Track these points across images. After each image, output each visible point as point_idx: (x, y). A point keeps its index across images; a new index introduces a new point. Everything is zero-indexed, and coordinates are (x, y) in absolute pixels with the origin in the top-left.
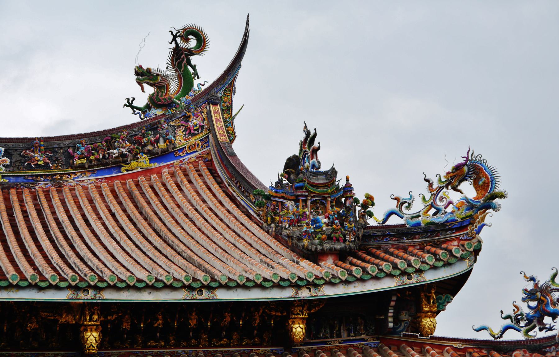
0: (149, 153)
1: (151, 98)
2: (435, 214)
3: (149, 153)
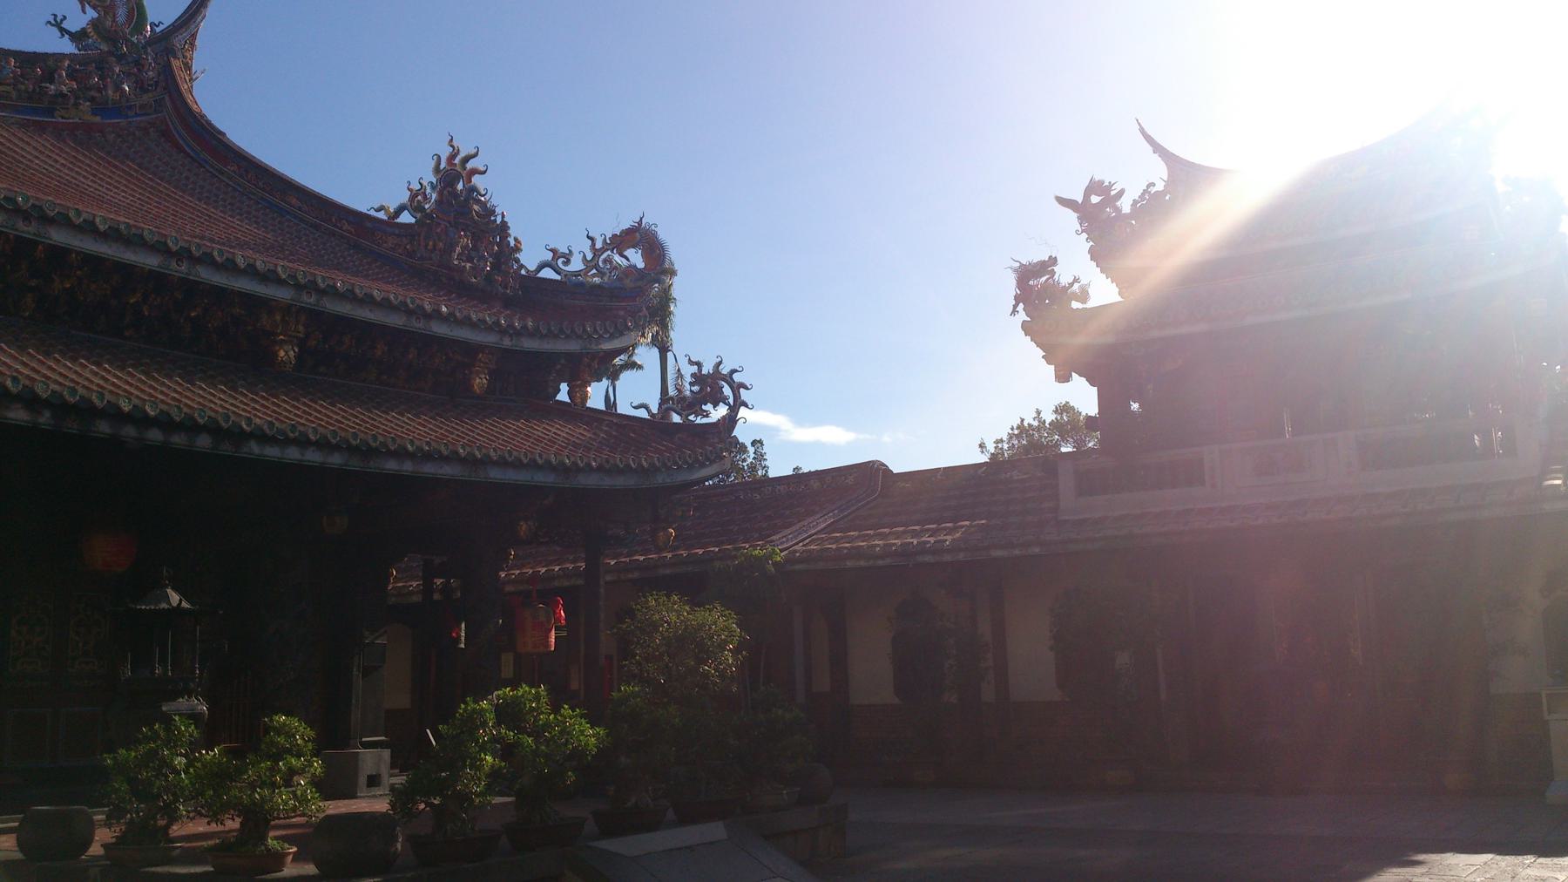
0: (92, 99)
1: (94, 23)
2: (594, 275)
3: (92, 99)
